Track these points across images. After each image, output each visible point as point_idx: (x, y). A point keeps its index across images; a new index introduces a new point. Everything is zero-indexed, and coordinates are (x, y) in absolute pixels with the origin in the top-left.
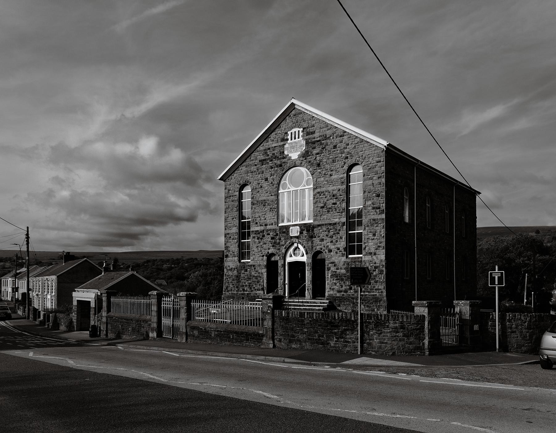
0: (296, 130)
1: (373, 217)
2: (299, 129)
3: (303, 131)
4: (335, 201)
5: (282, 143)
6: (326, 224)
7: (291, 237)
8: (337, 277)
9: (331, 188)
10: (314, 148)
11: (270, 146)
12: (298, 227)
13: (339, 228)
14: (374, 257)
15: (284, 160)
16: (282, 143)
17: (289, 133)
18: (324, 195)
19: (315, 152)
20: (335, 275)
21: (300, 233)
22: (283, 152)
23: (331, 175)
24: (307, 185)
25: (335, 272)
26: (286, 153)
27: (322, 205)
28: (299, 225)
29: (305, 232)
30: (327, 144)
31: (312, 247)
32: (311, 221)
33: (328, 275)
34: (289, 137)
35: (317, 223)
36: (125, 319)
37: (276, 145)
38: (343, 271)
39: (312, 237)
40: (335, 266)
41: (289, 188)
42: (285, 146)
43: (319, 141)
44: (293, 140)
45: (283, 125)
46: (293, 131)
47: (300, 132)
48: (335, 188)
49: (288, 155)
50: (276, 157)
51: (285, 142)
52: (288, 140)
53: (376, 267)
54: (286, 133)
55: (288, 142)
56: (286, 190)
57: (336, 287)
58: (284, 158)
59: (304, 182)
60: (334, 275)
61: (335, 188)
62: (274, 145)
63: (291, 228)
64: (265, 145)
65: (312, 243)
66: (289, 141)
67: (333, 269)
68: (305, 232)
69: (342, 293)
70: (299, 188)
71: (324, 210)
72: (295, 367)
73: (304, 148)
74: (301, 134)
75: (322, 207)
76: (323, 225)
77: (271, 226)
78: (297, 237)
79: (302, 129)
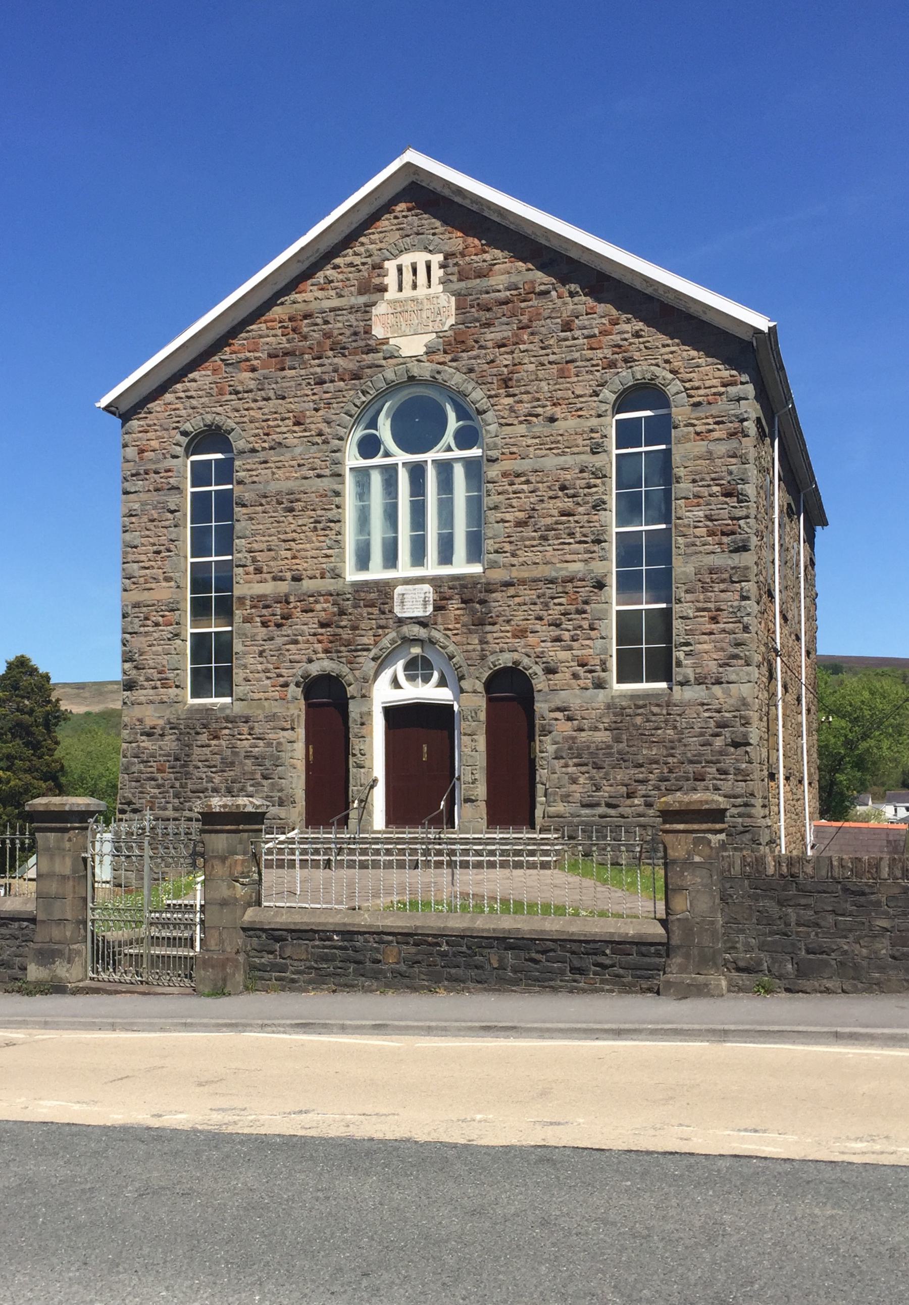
0: (420, 258)
1: (710, 560)
2: (429, 257)
3: (443, 266)
4: (568, 504)
5: (362, 300)
6: (535, 580)
7: (401, 621)
8: (579, 756)
9: (551, 462)
10: (488, 325)
11: (314, 306)
12: (427, 587)
13: (584, 592)
14: (717, 690)
15: (369, 358)
16: (362, 300)
17: (391, 266)
18: (528, 482)
19: (491, 336)
20: (573, 751)
21: (437, 608)
22: (368, 331)
23: (552, 420)
24: (461, 447)
25: (574, 739)
26: (378, 331)
27: (521, 515)
28: (436, 582)
29: (454, 605)
30: (538, 316)
31: (483, 658)
32: (476, 569)
33: (546, 747)
34: (391, 280)
35: (498, 575)
36: (251, 1025)
37: (336, 303)
38: (603, 737)
39: (480, 622)
40: (569, 719)
41: (387, 454)
42: (375, 311)
43: (506, 302)
44: (408, 292)
45: (369, 242)
46: (406, 259)
47: (435, 267)
48: (568, 460)
49: (385, 342)
50: (340, 349)
51: (375, 297)
52: (383, 289)
53: (722, 725)
54: (378, 267)
55: (387, 296)
56: (378, 460)
57: (578, 791)
58: (370, 350)
59: (449, 438)
60: (573, 751)
61: (568, 460)
62: (327, 304)
63: (399, 590)
64: (310, 296)
65: (483, 642)
66: (392, 293)
67: (563, 728)
68: (454, 605)
69: (602, 810)
70: (429, 457)
71: (528, 532)
72: (859, 1146)
73: (452, 321)
74: (437, 273)
75: (520, 524)
76: (523, 582)
77: (319, 581)
78: (422, 623)
79: (440, 257)
